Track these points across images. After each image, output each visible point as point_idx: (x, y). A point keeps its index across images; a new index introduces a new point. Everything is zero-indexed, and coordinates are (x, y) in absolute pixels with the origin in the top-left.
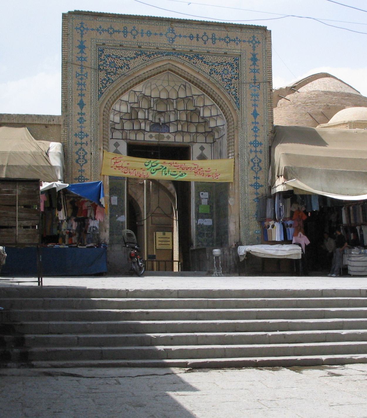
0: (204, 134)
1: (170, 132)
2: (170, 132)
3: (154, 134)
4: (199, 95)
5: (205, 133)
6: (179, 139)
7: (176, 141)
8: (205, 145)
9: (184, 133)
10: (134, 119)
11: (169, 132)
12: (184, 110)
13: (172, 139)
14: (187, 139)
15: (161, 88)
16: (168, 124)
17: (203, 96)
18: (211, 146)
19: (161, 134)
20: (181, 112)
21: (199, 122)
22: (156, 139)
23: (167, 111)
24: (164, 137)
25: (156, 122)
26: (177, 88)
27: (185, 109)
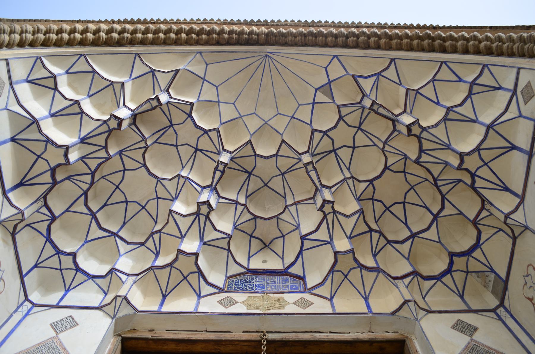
0: (447, 279)
1: (309, 286)
2: (309, 286)
3: (240, 297)
4: (378, 74)
5: (449, 271)
6: (349, 303)
7: (337, 312)
8: (469, 318)
9: (370, 277)
10: (159, 231)
11: (306, 290)
12: (345, 179)
13: (320, 306)
14: (386, 300)
15: (254, 124)
16: (296, 270)
17: (391, 73)
18: (500, 318)
19: (271, 295)
20: (333, 189)
21: (413, 236)
22: (248, 307)
23: (287, 206)
24: (285, 303)
25: (252, 266)
26: (304, 114)
27: (348, 175)
